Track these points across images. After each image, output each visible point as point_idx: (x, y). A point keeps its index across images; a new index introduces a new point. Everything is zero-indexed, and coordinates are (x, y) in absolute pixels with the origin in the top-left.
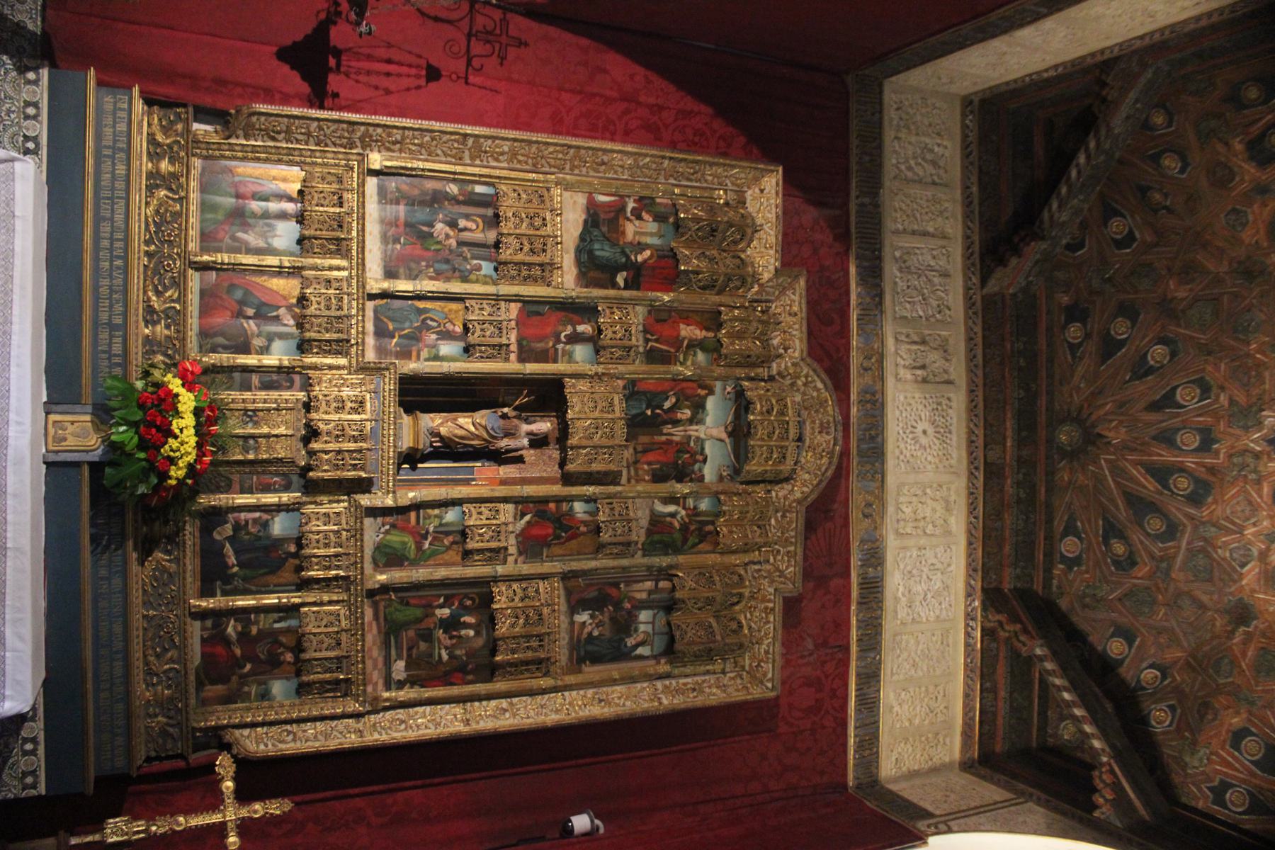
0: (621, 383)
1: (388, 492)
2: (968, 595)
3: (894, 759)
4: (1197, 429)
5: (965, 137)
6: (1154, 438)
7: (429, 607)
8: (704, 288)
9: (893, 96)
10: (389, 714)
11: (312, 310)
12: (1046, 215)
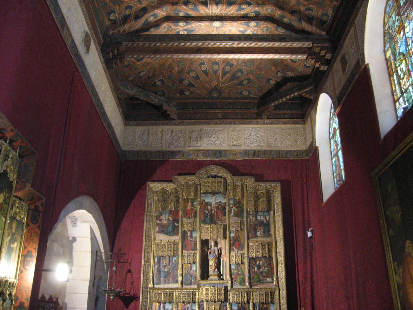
0: (202, 225)
1: (227, 282)
2: (258, 124)
3: (301, 145)
4: (213, 66)
5: (135, 125)
6: (215, 74)
7: (255, 272)
8: (178, 203)
9: (126, 147)
10: (279, 282)
11: (186, 300)
12: (156, 104)
